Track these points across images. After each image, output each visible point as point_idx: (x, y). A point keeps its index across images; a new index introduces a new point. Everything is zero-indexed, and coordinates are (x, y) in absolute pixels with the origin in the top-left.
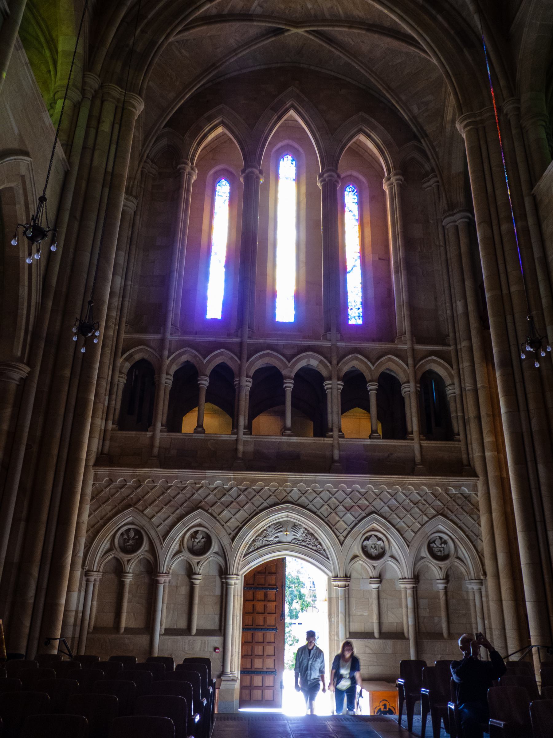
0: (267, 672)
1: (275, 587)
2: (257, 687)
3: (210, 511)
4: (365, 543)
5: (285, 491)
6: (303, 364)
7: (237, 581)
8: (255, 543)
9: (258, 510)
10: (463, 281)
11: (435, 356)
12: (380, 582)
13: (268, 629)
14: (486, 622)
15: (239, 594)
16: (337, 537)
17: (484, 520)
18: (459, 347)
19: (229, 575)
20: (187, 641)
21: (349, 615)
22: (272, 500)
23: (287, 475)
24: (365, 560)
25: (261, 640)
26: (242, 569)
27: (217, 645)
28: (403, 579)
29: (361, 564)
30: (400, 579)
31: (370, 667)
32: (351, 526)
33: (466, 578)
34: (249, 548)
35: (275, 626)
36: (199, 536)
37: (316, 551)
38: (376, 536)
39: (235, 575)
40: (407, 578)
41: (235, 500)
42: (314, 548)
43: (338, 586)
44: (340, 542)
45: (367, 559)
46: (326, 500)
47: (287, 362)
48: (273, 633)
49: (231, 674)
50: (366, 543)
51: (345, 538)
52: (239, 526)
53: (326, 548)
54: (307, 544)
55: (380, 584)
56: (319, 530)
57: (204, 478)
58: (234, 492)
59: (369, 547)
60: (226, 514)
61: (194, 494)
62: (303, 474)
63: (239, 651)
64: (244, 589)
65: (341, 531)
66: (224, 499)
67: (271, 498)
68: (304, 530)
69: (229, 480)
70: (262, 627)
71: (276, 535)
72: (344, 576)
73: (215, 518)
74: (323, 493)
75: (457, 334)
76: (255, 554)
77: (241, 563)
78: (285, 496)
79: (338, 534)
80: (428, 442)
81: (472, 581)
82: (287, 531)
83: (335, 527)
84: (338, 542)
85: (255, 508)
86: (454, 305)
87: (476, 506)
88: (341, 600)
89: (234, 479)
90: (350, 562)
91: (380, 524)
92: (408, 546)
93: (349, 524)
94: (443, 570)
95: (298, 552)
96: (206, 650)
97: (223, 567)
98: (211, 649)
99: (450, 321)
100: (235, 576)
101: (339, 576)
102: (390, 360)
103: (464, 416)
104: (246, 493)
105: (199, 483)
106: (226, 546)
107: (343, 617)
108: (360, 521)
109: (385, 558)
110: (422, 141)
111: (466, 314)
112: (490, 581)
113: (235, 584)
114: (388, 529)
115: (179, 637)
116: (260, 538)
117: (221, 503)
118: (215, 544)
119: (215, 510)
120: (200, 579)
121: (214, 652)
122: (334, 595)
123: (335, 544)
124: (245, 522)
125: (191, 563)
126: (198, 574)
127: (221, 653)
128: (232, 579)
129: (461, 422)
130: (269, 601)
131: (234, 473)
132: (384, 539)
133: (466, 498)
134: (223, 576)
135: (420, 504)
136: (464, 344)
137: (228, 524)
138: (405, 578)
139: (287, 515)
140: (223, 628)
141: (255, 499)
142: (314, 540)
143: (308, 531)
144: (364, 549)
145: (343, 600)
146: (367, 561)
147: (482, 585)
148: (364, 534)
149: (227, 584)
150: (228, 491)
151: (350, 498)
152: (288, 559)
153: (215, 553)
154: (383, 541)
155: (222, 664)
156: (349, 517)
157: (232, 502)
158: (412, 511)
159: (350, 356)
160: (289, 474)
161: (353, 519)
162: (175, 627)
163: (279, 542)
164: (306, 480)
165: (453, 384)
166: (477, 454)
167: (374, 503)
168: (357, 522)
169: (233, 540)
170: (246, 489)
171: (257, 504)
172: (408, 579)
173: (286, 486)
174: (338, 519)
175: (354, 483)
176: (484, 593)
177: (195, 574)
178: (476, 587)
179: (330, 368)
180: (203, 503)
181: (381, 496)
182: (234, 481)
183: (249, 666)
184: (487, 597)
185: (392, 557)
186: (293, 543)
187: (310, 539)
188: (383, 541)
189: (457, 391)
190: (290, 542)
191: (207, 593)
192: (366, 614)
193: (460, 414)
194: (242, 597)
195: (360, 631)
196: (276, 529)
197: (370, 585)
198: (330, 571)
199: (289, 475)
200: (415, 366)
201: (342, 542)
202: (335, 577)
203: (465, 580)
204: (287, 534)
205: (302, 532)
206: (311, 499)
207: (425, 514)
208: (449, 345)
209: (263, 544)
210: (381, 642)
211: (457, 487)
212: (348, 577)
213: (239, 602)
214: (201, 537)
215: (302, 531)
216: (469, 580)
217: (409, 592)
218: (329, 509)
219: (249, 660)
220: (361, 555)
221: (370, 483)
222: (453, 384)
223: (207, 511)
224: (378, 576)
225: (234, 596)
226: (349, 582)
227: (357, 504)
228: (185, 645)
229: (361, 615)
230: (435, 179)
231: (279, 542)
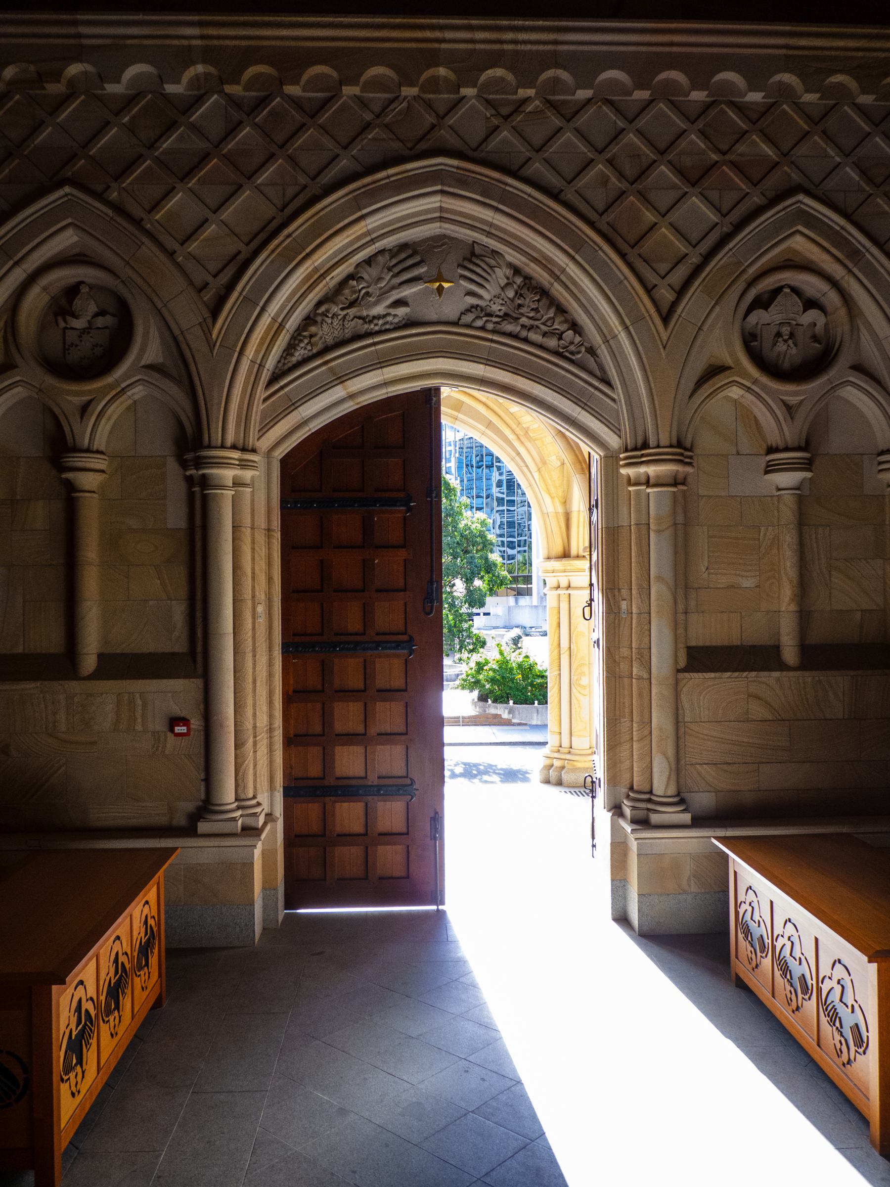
0: (379, 787)
1: (402, 495)
2: (347, 838)
3: (114, 195)
4: (753, 319)
5: (429, 105)
7: (248, 475)
8: (313, 329)
12: (808, 465)
13: (378, 644)
15: (262, 522)
16: (649, 291)
19: (210, 447)
20: (62, 697)
21: (687, 588)
23: (432, 27)
24: (755, 382)
25: (356, 682)
26: (264, 430)
27: (177, 710)
29: (735, 402)
32: (704, 247)
34: (291, 348)
35: (405, 634)
36: (88, 307)
38: (796, 291)
39: (234, 447)
41: (217, 146)
42: (552, 343)
43: (648, 483)
44: (658, 311)
45: (764, 379)
46: (600, 142)
48: (398, 656)
49: (238, 808)
50: (759, 317)
51: (681, 292)
52: (239, 252)
53: (596, 338)
54: (523, 326)
55: (809, 470)
56: (573, 270)
59: (768, 335)
61: (36, 129)
62: (505, 23)
63: (271, 724)
64: (282, 508)
65: (663, 267)
68: (509, 272)
69: (186, 57)
70: (358, 638)
71: (395, 295)
72: (674, 442)
73: (137, 223)
74: (592, 110)
76: (317, 370)
77: (258, 407)
79: (652, 278)
82: (440, 278)
83: (636, 250)
84: (652, 310)
85: (302, 180)
88: (658, 532)
89: (208, 55)
91: (821, 233)
93: (695, 236)
95: (488, 362)
96: (139, 728)
97: (186, 423)
98: (159, 725)
100: (236, 455)
101: (652, 442)
105: (56, 76)
106: (188, 337)
107: (668, 596)
108: (738, 227)
109: (833, 372)
113: (238, 483)
114: (855, 254)
115: (30, 686)
116: (335, 309)
117: (157, 160)
118: (146, 333)
120: (103, 471)
121: (170, 734)
122: (628, 517)
123: (638, 319)
124: (263, 236)
125: (56, 410)
126: (88, 450)
127: (197, 738)
128: (223, 463)
130: (378, 547)
131: (200, 24)
134: (189, 456)
137: (193, 247)
139: (441, 209)
140: (199, 648)
142: (551, 314)
143: (527, 278)
144: (750, 341)
145: (668, 533)
146: (764, 388)
148: (751, 284)
149: (205, 482)
150: (184, 113)
151: (703, 134)
152: (445, 391)
153: (151, 367)
154: (822, 309)
155: (203, 776)
157: (205, 158)
161: (713, 217)
162: (20, 650)
163: (410, 323)
164: (516, 52)
167: (802, 150)
168: (726, 229)
169: (215, 312)
170: (262, 102)
173: (434, 85)
174: (650, 217)
175: (722, 63)
177: (77, 449)
182: (204, 61)
183: (315, 770)
185: (859, 368)
186: (468, 326)
187: (536, 310)
188: (822, 309)
192: (748, 583)
194: (278, 535)
195: (726, 643)
196: (396, 270)
197: (769, 477)
198: (617, 431)
201: (665, 310)
202: (635, 449)
205: (503, 282)
206: (537, 139)
209: (348, 333)
210: (810, 679)
212: (686, 449)
213: (262, 552)
214: (93, 308)
215: (501, 275)
219: (314, 752)
221: (789, 63)
223: (99, 196)
224: (803, 444)
225: (236, 528)
226: (690, 464)
227: (731, 157)
228: (55, 714)
229: (733, 587)
231: (410, 323)
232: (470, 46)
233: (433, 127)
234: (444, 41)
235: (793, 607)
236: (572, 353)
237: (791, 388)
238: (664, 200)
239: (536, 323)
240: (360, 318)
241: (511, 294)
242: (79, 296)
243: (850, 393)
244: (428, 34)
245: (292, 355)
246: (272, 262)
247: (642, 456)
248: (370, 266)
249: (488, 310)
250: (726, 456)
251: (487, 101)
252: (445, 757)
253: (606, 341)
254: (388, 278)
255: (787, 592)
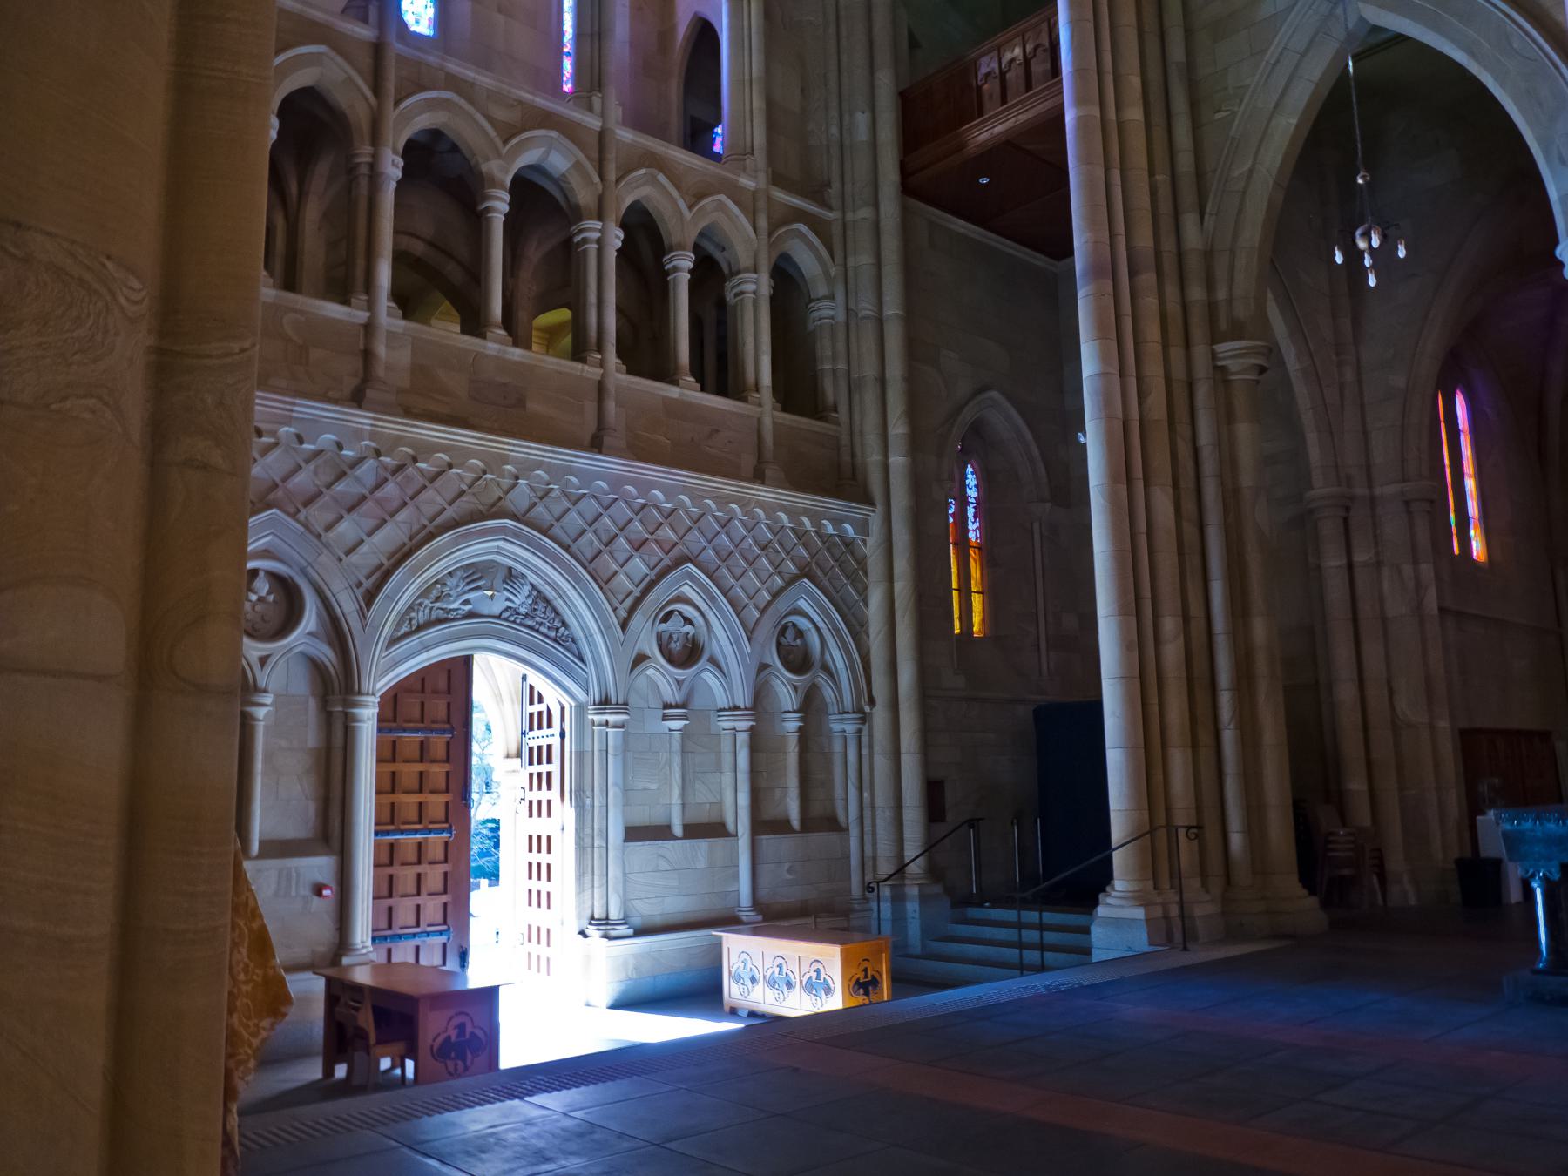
6: (529, 157)
8: (413, 615)
9: (431, 527)
14: (865, 795)
17: (876, 598)
22: (465, 503)
24: (662, 666)
28: (730, 709)
30: (721, 710)
31: (667, 900)
33: (833, 709)
34: (399, 625)
37: (555, 640)
38: (680, 613)
40: (742, 707)
42: (553, 634)
45: (668, 666)
47: (498, 141)
53: (579, 634)
54: (537, 622)
55: (687, 720)
57: (288, 421)
58: (368, 470)
60: (347, 528)
65: (621, 597)
66: (340, 487)
67: (464, 498)
75: (848, 187)
78: (496, 497)
79: (616, 604)
80: (787, 416)
81: (846, 716)
86: (846, 118)
87: (862, 562)
90: (631, 672)
92: (749, 639)
94: (800, 691)
95: (515, 643)
96: (293, 893)
98: (306, 891)
99: (835, 151)
101: (613, 701)
102: (721, 204)
103: (849, 371)
104: (400, 477)
112: (880, 716)
114: (713, 599)
116: (427, 602)
119: (318, 515)
121: (316, 899)
123: (608, 628)
129: (843, 384)
131: (375, 419)
132: (699, 620)
133: (847, 545)
135: (771, 550)
136: (865, 213)
138: (736, 708)
141: (424, 496)
143: (539, 592)
146: (666, 670)
147: (864, 723)
151: (641, 522)
153: (310, 634)
156: (639, 566)
157: (364, 498)
158: (757, 565)
159: (643, 171)
160: (515, 442)
161: (646, 570)
163: (471, 615)
165: (831, 297)
168: (653, 577)
169: (369, 604)
171: (429, 510)
172: (746, 709)
176: (865, 739)
178: (850, 728)
179: (600, 187)
180: (279, 493)
181: (702, 523)
182: (370, 440)
184: (871, 747)
185: (713, 661)
186: (506, 620)
187: (544, 613)
190: (499, 617)
191: (284, 743)
192: (653, 787)
193: (842, 366)
195: (648, 824)
199: (514, 445)
200: (770, 235)
202: (600, 704)
203: (827, 713)
204: (492, 597)
205: (527, 593)
207: (780, 574)
208: (830, 208)
210: (688, 845)
211: (837, 522)
216: (840, 713)
217: (743, 738)
218: (596, 542)
220: (656, 658)
221: (685, 490)
222: (831, 297)
227: (654, 537)
229: (645, 789)
231: (471, 615)
232: (526, 456)
233: (500, 498)
234: (512, 451)
235: (679, 801)
236: (563, 641)
237: (680, 671)
238: (622, 557)
239: (544, 621)
240: (442, 609)
241: (530, 601)
242: (258, 579)
243: (707, 676)
244: (506, 447)
245: (399, 631)
246: (404, 574)
247: (605, 709)
248: (452, 577)
249: (517, 610)
250: (642, 709)
251: (530, 487)
252: (473, 909)
253: (586, 637)
254: (462, 586)
255: (676, 792)
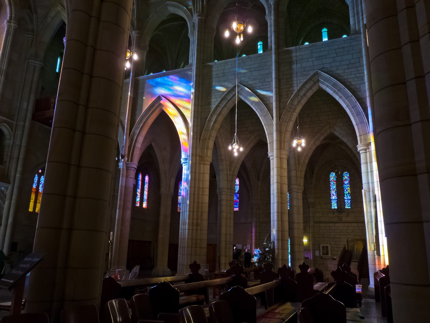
10: (30, 93)
11: (6, 123)
17: (7, 203)
18: (18, 123)
87: (5, 196)
110: (34, 15)
111: (27, 110)
136: (22, 123)
166: (12, 174)
189: (11, 143)
193: (9, 154)
208: (14, 121)
222: (10, 139)
230: (32, 36)
